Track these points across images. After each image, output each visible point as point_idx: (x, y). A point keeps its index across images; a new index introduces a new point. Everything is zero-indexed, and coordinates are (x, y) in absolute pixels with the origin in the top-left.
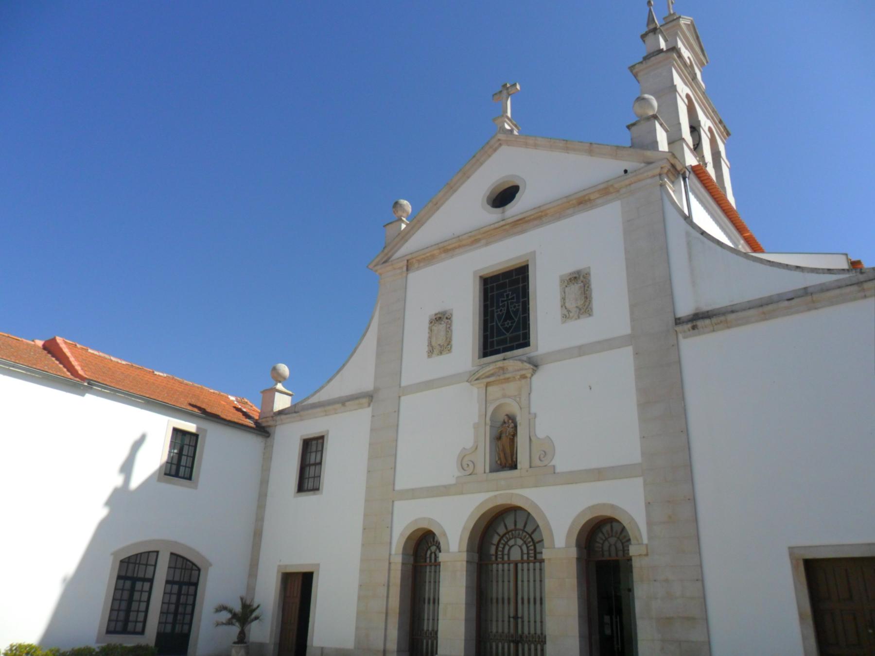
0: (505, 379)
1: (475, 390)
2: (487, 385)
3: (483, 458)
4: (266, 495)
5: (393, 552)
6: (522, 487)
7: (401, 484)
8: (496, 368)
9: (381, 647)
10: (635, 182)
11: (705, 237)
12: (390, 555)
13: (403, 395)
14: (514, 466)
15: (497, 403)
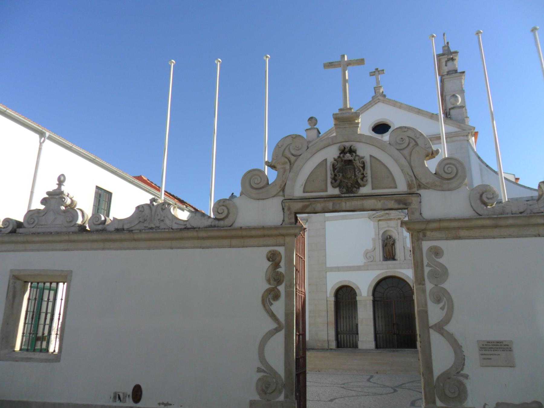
0: (389, 219)
1: (372, 223)
2: (378, 221)
3: (379, 253)
4: (339, 271)
5: (328, 296)
6: (401, 268)
7: (329, 265)
8: (385, 213)
9: (326, 339)
10: (455, 137)
11: (488, 168)
12: (327, 297)
13: (328, 221)
14: (394, 259)
15: (385, 229)
